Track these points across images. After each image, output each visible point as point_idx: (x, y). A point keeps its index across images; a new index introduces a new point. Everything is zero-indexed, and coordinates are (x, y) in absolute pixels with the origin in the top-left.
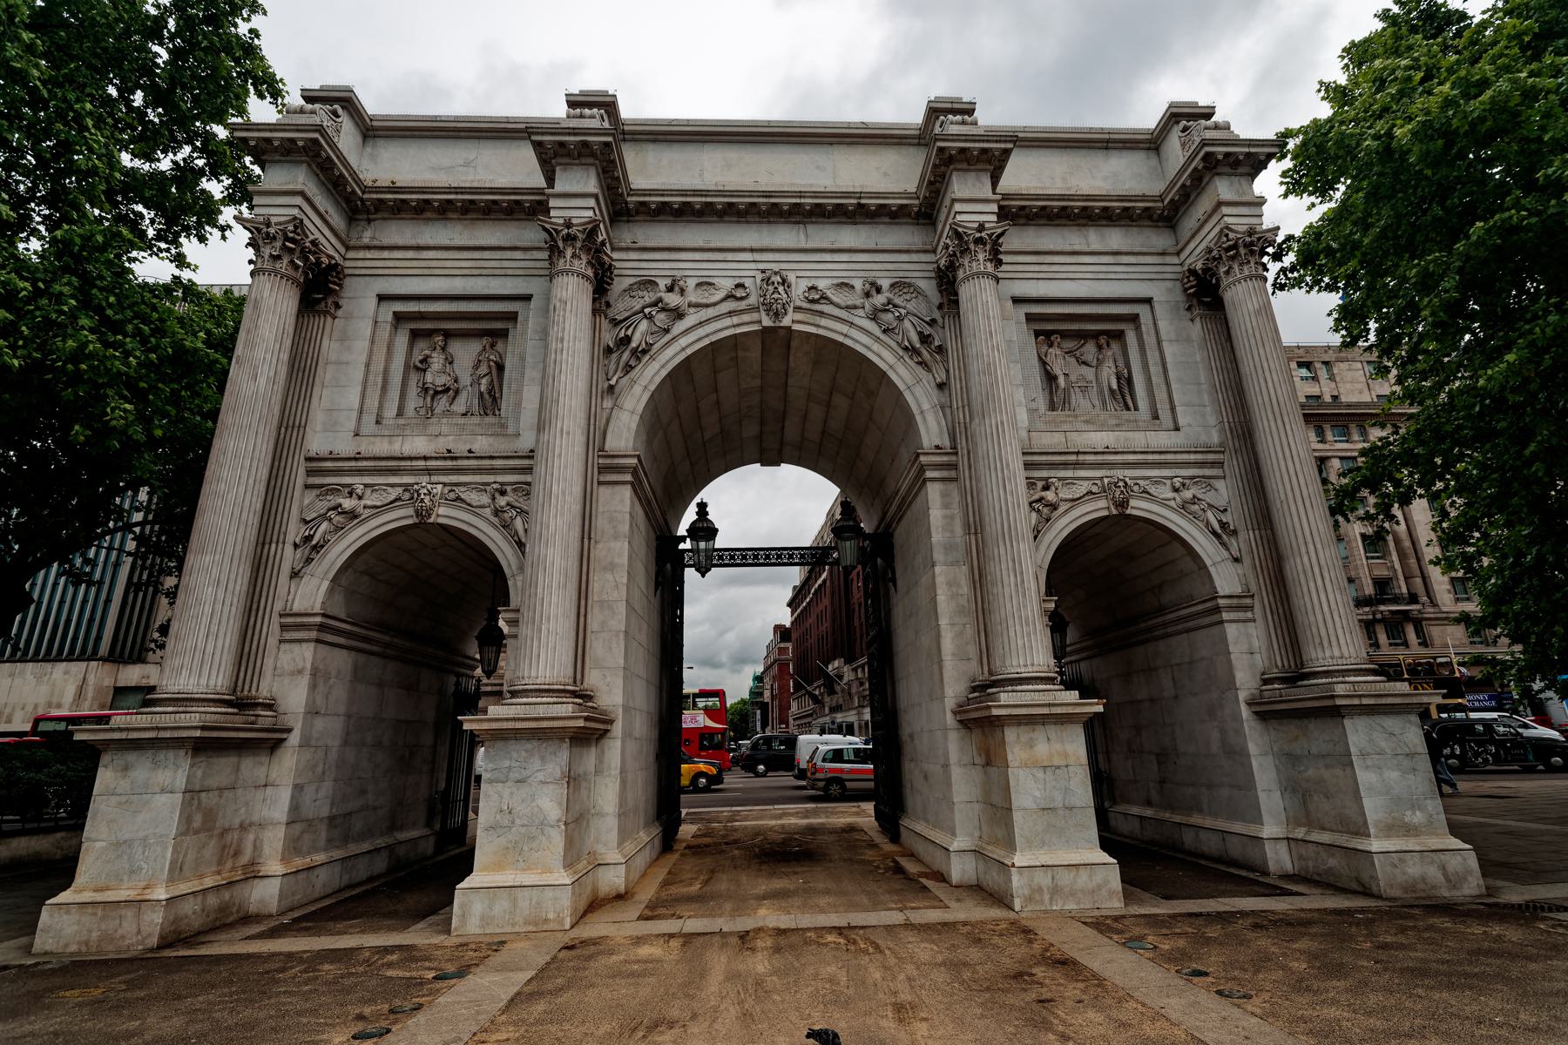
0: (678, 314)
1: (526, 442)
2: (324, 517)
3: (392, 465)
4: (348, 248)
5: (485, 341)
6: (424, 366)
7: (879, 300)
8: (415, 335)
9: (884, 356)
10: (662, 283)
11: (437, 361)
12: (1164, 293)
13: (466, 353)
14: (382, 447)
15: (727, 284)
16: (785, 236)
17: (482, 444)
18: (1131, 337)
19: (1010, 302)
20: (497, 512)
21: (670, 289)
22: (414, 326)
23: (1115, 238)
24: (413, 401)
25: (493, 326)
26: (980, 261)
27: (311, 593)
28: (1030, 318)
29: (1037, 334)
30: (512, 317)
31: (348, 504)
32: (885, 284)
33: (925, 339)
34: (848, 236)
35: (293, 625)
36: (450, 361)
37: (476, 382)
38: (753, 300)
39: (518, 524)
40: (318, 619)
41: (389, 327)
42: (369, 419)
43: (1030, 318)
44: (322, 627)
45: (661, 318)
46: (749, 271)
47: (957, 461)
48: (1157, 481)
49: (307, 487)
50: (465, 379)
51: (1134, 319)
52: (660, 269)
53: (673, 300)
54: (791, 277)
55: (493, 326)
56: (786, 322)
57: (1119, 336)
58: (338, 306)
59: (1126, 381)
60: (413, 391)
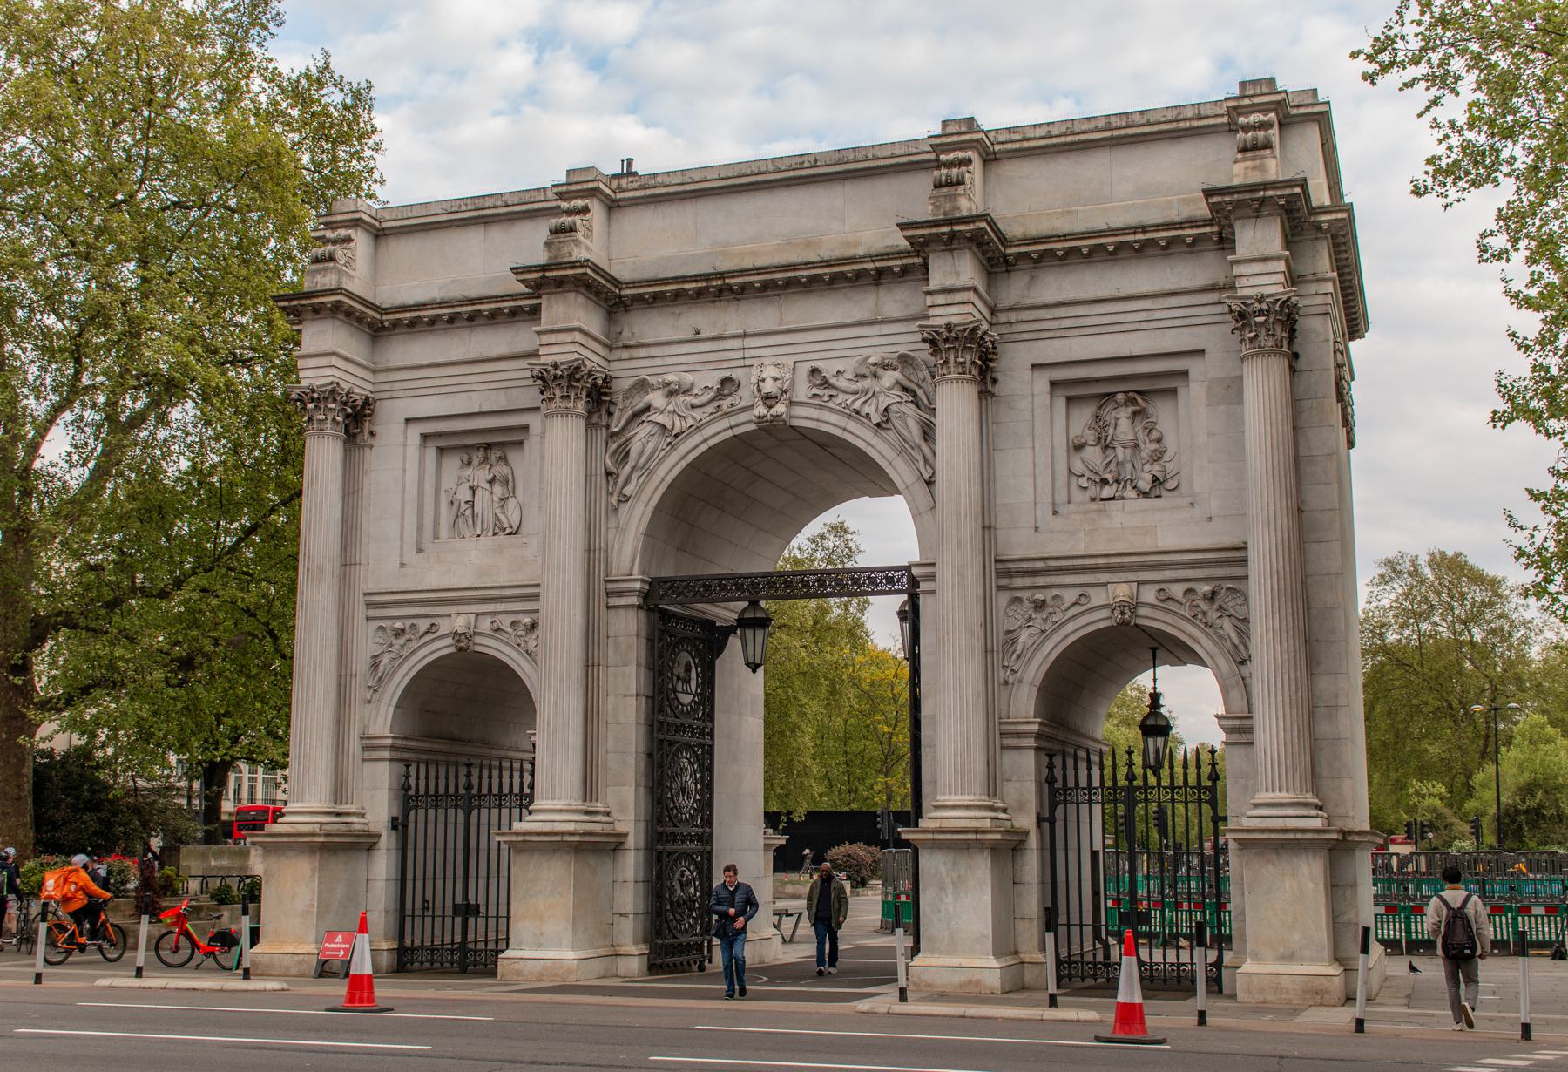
4: (374, 372)
8: (441, 450)
18: (1181, 392)
19: (1028, 374)
22: (443, 443)
27: (381, 719)
28: (1053, 384)
29: (1070, 400)
30: (526, 428)
35: (370, 746)
40: (389, 741)
41: (417, 454)
42: (410, 548)
43: (1053, 384)
44: (393, 748)
49: (368, 619)
51: (1184, 374)
57: (1174, 391)
58: (372, 434)
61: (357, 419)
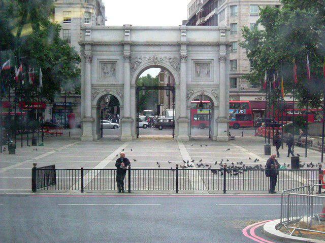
1: (120, 83)
2: (95, 93)
6: (103, 69)
10: (138, 57)
11: (105, 68)
12: (216, 59)
13: (109, 66)
14: (101, 83)
16: (156, 49)
17: (114, 83)
19: (191, 61)
20: (117, 93)
21: (140, 59)
23: (210, 48)
24: (103, 74)
26: (183, 61)
27: (95, 103)
33: (177, 67)
34: (167, 48)
36: (107, 68)
37: (111, 71)
42: (98, 78)
45: (138, 64)
46: (151, 55)
47: (179, 87)
52: (138, 55)
53: (140, 61)
54: (158, 57)
55: (113, 63)
59: (208, 72)
61: (91, 59)
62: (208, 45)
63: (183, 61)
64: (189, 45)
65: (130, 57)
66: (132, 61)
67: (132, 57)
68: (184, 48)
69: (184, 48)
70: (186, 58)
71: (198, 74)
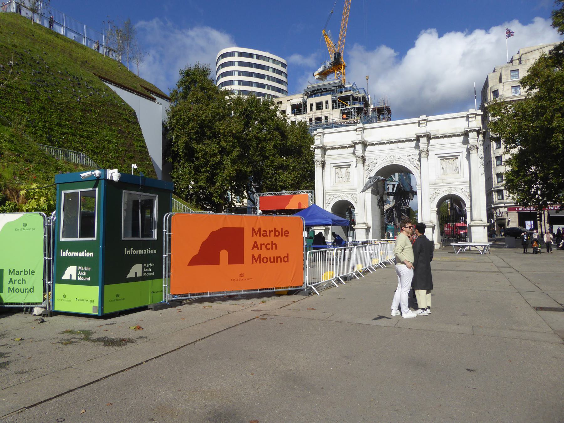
0: (376, 163)
3: (336, 191)
5: (345, 169)
7: (410, 158)
9: (410, 167)
10: (374, 158)
11: (340, 173)
13: (344, 170)
15: (384, 157)
24: (337, 179)
25: (348, 166)
31: (332, 197)
32: (411, 154)
37: (346, 176)
38: (388, 159)
39: (355, 200)
43: (438, 157)
48: (458, 188)
50: (344, 175)
53: (375, 161)
55: (348, 166)
56: (394, 163)
60: (337, 178)
61: (323, 164)
62: (454, 136)
63: (424, 155)
64: (429, 137)
65: (364, 159)
66: (367, 162)
67: (367, 158)
68: (423, 140)
69: (423, 140)
70: (428, 153)
71: (445, 173)
